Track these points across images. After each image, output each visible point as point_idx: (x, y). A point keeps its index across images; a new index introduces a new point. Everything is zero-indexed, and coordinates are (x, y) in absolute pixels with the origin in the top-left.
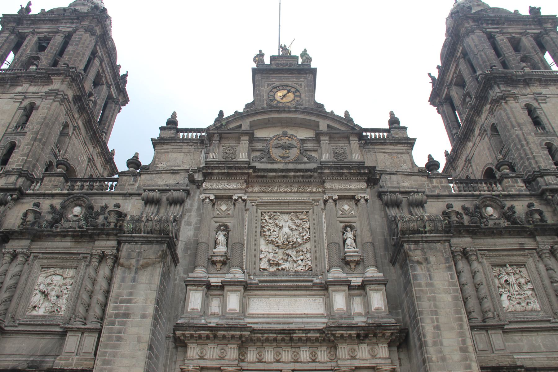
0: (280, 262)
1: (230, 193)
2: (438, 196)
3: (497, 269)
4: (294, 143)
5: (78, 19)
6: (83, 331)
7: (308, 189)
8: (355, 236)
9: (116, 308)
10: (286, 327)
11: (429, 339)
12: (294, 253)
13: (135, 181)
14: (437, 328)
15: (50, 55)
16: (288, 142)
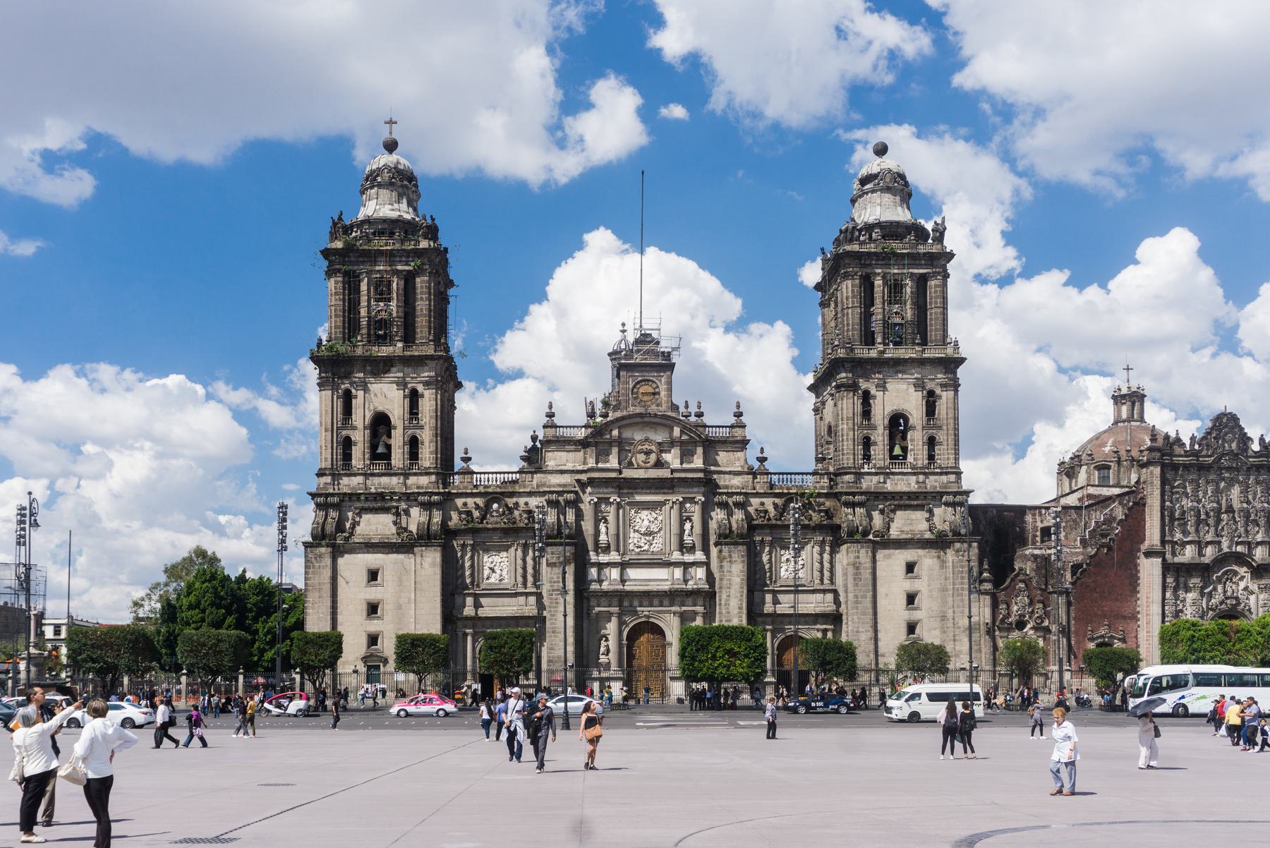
0: (642, 545)
1: (608, 496)
2: (757, 495)
3: (783, 552)
4: (653, 448)
5: (415, 253)
6: (527, 595)
7: (662, 491)
8: (692, 527)
9: (551, 586)
10: (646, 588)
11: (723, 602)
12: (651, 538)
13: (533, 478)
14: (729, 596)
15: (400, 310)
16: (649, 448)
